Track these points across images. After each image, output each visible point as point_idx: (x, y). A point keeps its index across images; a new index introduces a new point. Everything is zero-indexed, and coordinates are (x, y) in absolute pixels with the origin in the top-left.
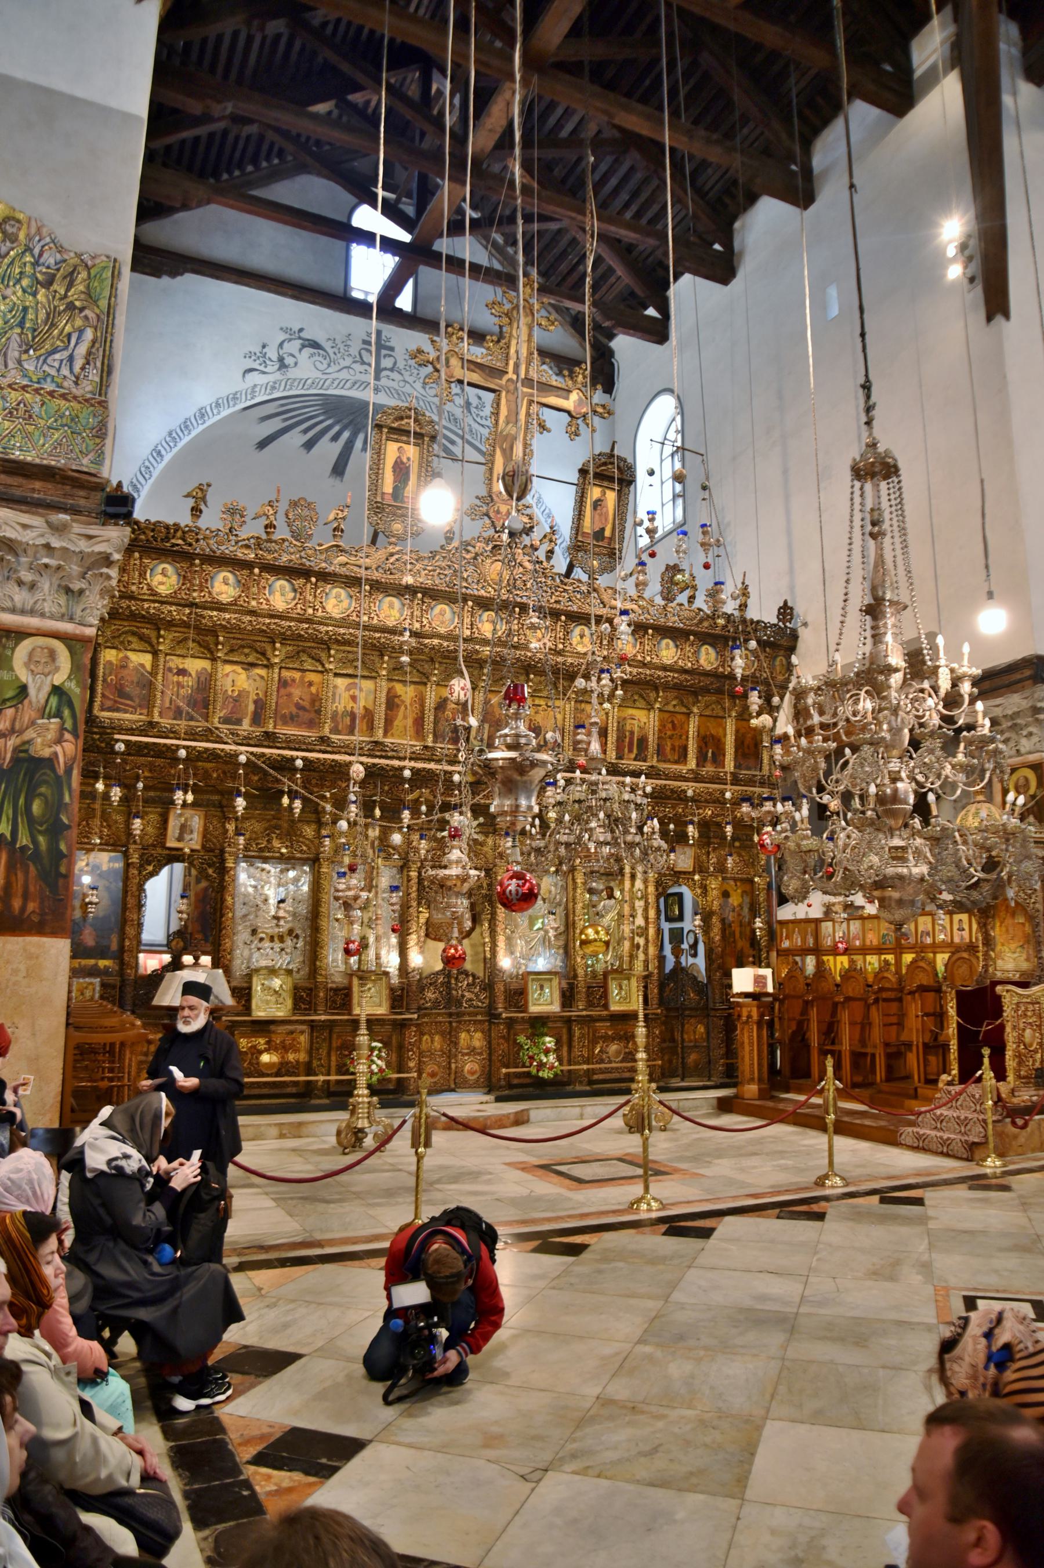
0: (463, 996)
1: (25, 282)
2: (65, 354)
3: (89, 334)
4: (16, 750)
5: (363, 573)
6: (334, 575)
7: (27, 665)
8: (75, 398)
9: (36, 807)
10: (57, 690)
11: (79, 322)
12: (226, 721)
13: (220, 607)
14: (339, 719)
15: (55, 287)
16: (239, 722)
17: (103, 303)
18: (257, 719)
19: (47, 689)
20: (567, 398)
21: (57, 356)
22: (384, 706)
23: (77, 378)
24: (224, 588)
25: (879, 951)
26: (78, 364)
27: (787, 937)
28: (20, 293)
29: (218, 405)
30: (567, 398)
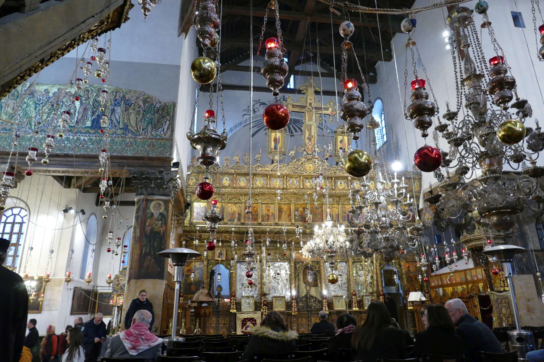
0: (312, 305)
1: (152, 112)
2: (162, 128)
3: (168, 123)
4: (150, 230)
5: (266, 173)
6: (258, 174)
7: (153, 208)
8: (165, 139)
9: (155, 244)
10: (161, 214)
11: (165, 120)
12: (230, 220)
13: (225, 187)
14: (264, 217)
15: (159, 112)
16: (233, 220)
17: (171, 114)
18: (239, 219)
19: (158, 214)
20: (328, 110)
21: (160, 129)
22: (278, 212)
23: (165, 134)
24: (226, 182)
25: (461, 284)
26: (165, 131)
27: (433, 282)
28: (151, 115)
29: (236, 126)
30: (328, 110)
